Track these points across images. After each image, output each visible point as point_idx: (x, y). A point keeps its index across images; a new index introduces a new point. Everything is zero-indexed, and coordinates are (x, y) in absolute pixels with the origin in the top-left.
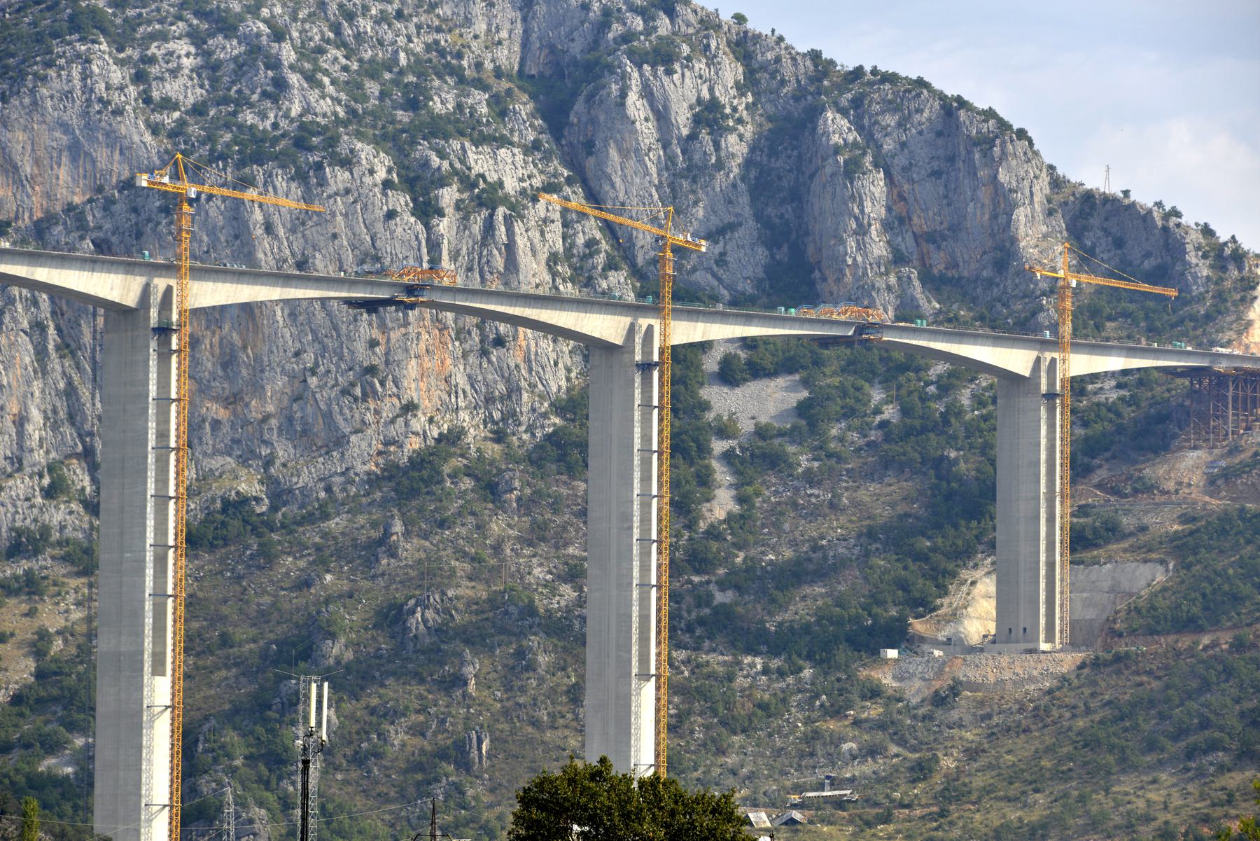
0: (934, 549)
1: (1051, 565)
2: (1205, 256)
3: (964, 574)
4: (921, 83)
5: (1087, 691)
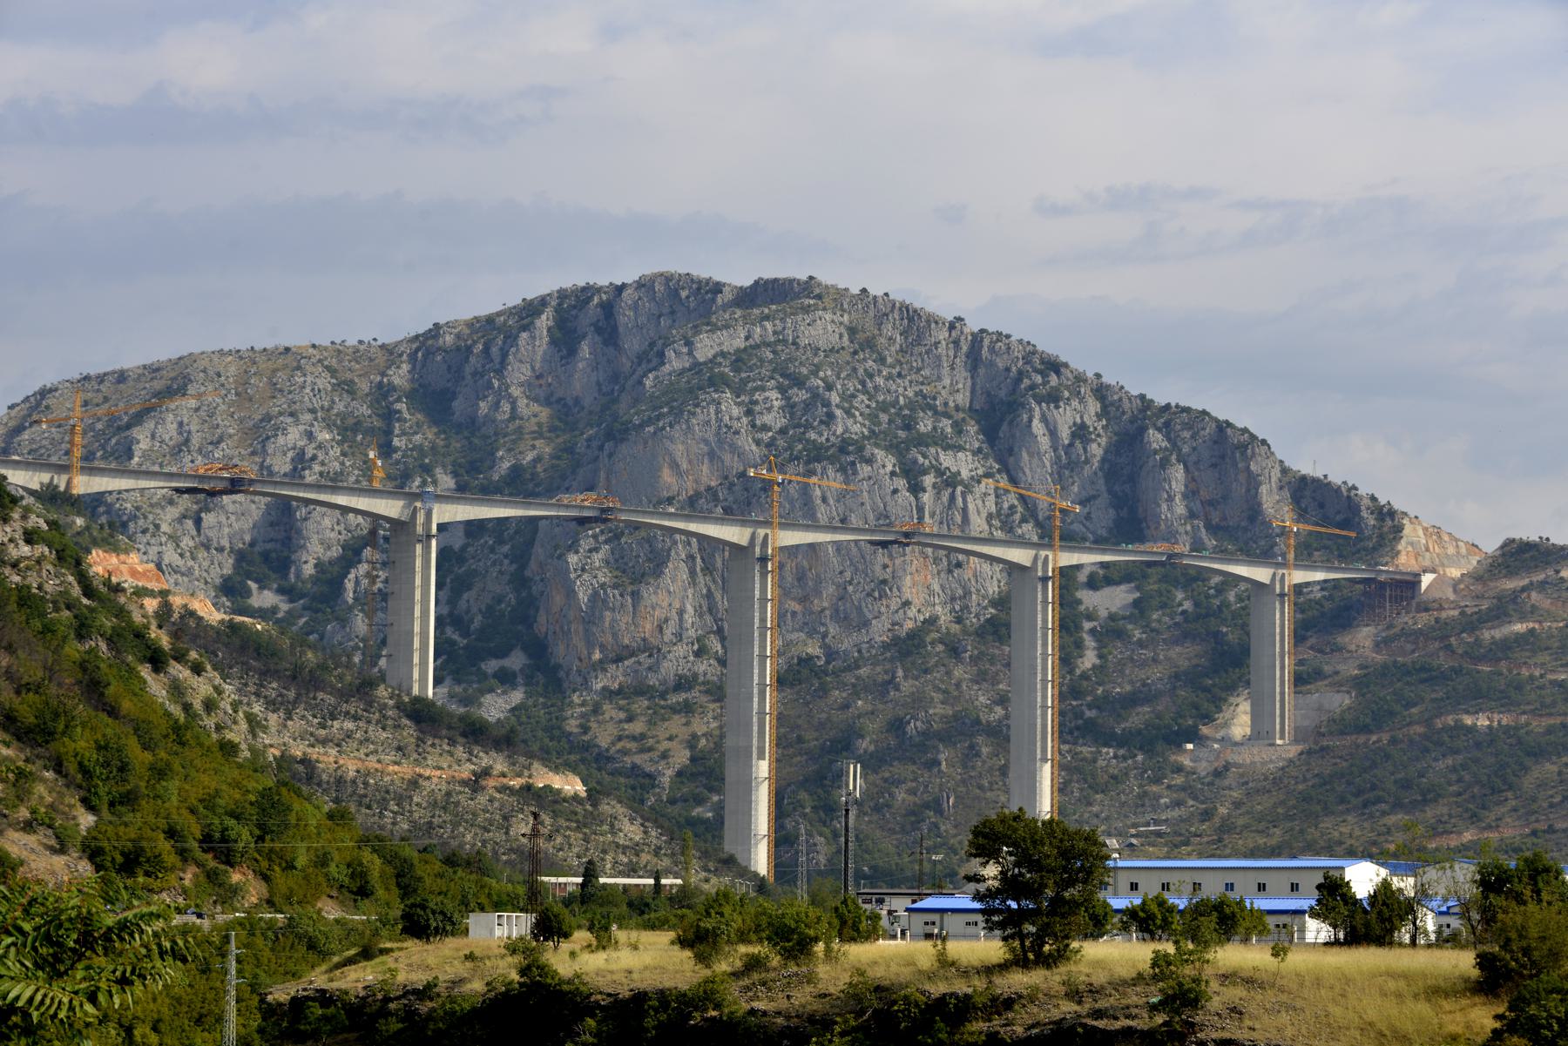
0: (1214, 685)
1: (1282, 693)
3: (1232, 700)
4: (1204, 413)
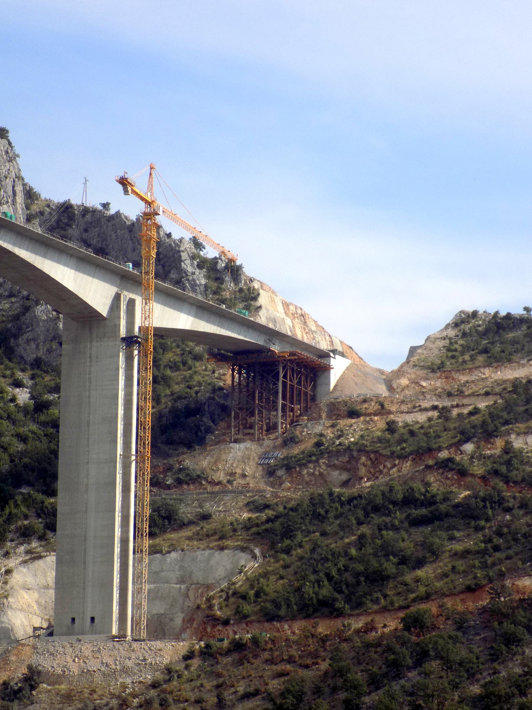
1: (124, 542)
2: (200, 266)
5: (209, 684)
